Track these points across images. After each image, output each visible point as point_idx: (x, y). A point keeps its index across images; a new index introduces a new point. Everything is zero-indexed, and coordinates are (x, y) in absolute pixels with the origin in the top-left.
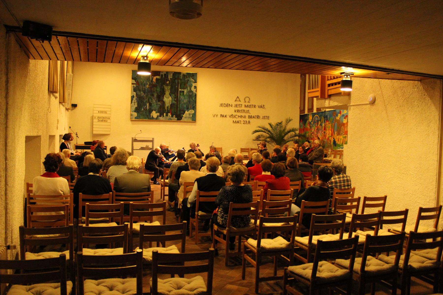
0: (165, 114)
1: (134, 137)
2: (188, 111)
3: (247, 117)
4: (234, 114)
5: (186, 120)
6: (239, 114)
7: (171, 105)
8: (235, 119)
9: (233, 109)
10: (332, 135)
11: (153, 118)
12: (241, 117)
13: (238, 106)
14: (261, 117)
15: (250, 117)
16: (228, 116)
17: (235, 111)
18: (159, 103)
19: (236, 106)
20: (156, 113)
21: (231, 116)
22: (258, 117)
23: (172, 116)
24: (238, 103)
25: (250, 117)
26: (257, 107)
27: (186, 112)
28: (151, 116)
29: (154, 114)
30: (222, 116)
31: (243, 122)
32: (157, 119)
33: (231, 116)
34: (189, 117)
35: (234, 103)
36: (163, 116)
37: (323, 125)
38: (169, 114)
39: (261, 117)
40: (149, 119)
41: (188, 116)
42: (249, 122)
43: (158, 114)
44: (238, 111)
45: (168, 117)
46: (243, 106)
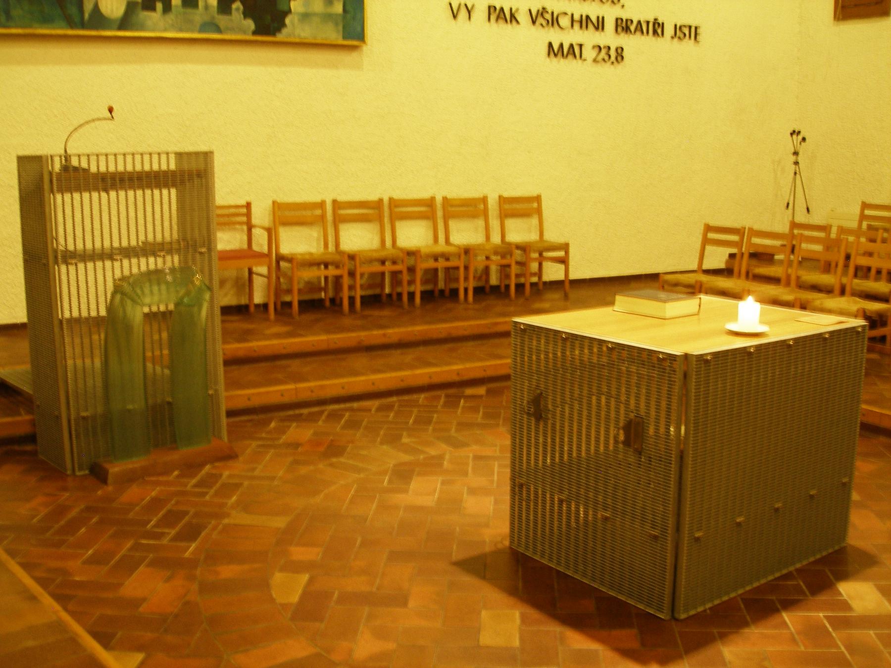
1: (48, 145)
3: (610, 25)
5: (305, 32)
11: (98, 20)
14: (669, 30)
15: (623, 26)
16: (523, 18)
22: (657, 28)
25: (623, 26)
28: (88, 7)
31: (593, 54)
33: (543, 18)
34: (328, 17)
36: (167, 8)
39: (669, 30)
40: (71, 25)
42: (620, 54)
45: (198, 15)
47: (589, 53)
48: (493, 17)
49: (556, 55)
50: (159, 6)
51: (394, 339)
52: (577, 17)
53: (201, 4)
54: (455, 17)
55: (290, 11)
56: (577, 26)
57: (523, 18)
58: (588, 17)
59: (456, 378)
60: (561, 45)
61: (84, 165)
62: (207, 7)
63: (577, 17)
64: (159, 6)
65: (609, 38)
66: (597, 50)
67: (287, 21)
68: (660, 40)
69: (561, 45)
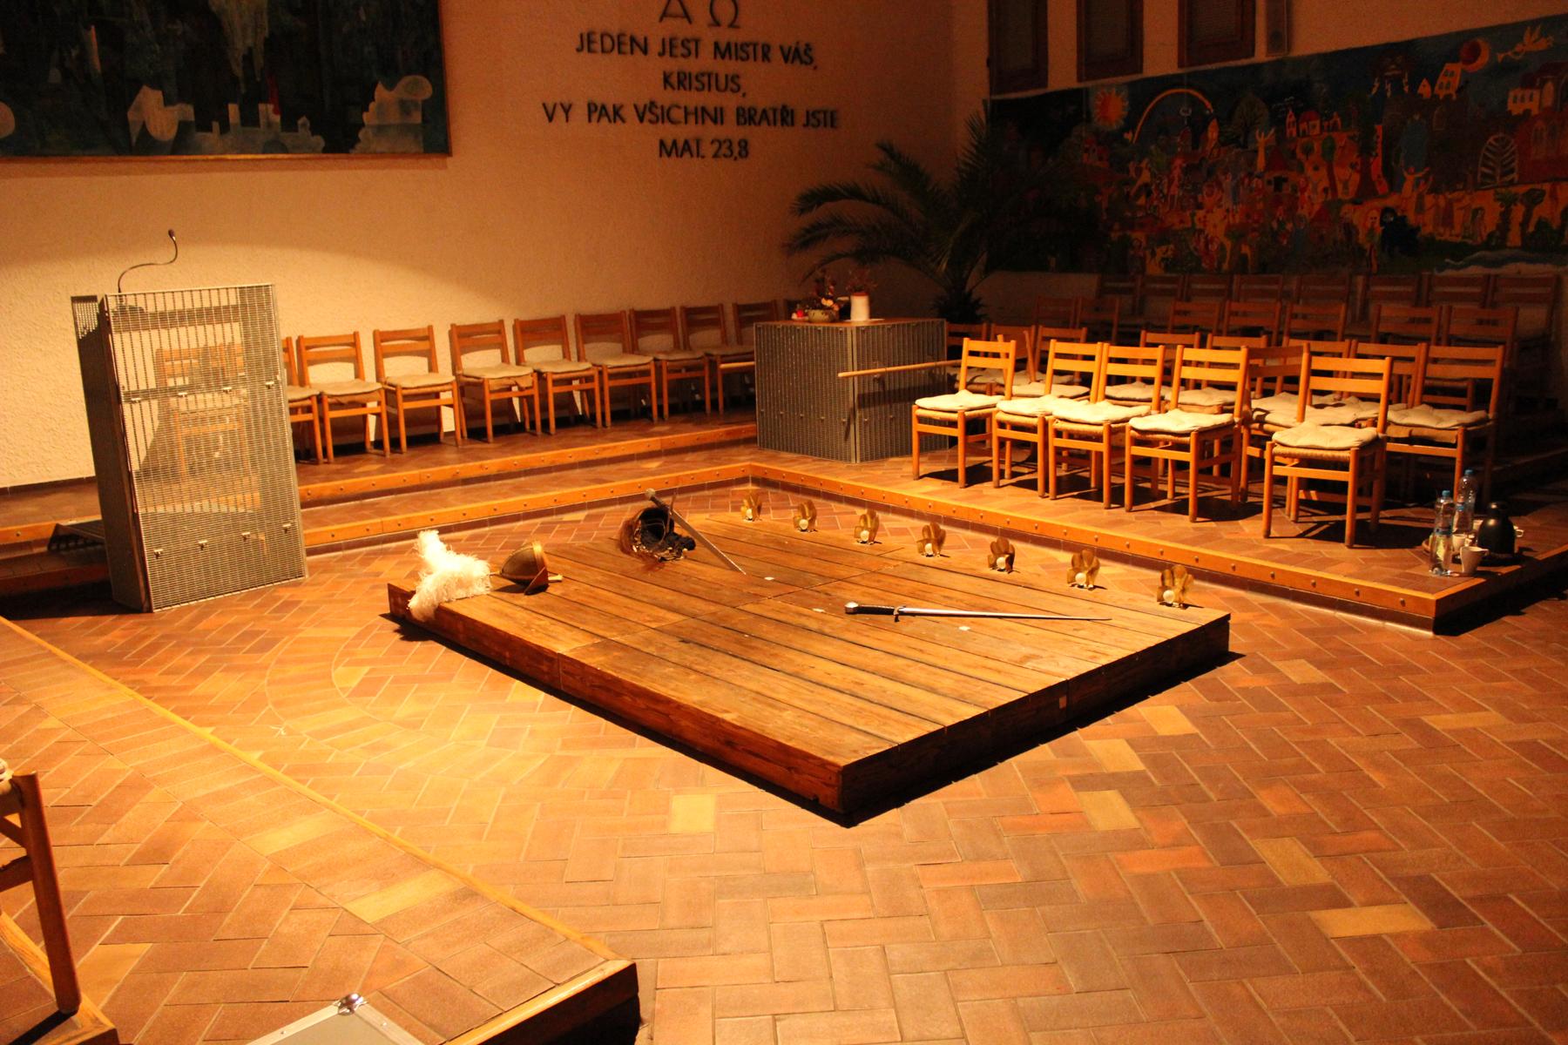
0: (233, 110)
2: (390, 86)
3: (731, 116)
4: (666, 97)
6: (692, 99)
7: (267, 42)
8: (669, 132)
9: (655, 66)
10: (1366, 192)
12: (702, 114)
13: (680, 50)
14: (800, 117)
15: (747, 116)
16: (629, 113)
17: (666, 80)
18: (179, 27)
19: (669, 47)
20: (168, 101)
21: (650, 112)
22: (785, 116)
23: (289, 124)
24: (678, 28)
25: (747, 116)
26: (776, 55)
27: (381, 92)
28: (135, 131)
29: (156, 112)
30: (597, 111)
32: (181, 145)
33: (650, 112)
34: (405, 129)
35: (657, 33)
36: (225, 128)
37: (1263, 139)
38: (267, 111)
39: (800, 117)
41: (394, 118)
42: (744, 145)
43: (188, 111)
44: (683, 81)
46: (707, 50)
47: (708, 150)
48: (595, 116)
49: (669, 155)
50: (216, 125)
51: (493, 470)
52: (691, 108)
53: (262, 121)
54: (551, 119)
55: (363, 125)
56: (692, 118)
57: (629, 113)
58: (703, 109)
59: (555, 506)
60: (675, 143)
61: (141, 304)
62: (269, 125)
63: (691, 108)
64: (216, 125)
65: (731, 130)
66: (716, 145)
67: (360, 135)
68: (788, 129)
69: (675, 143)
